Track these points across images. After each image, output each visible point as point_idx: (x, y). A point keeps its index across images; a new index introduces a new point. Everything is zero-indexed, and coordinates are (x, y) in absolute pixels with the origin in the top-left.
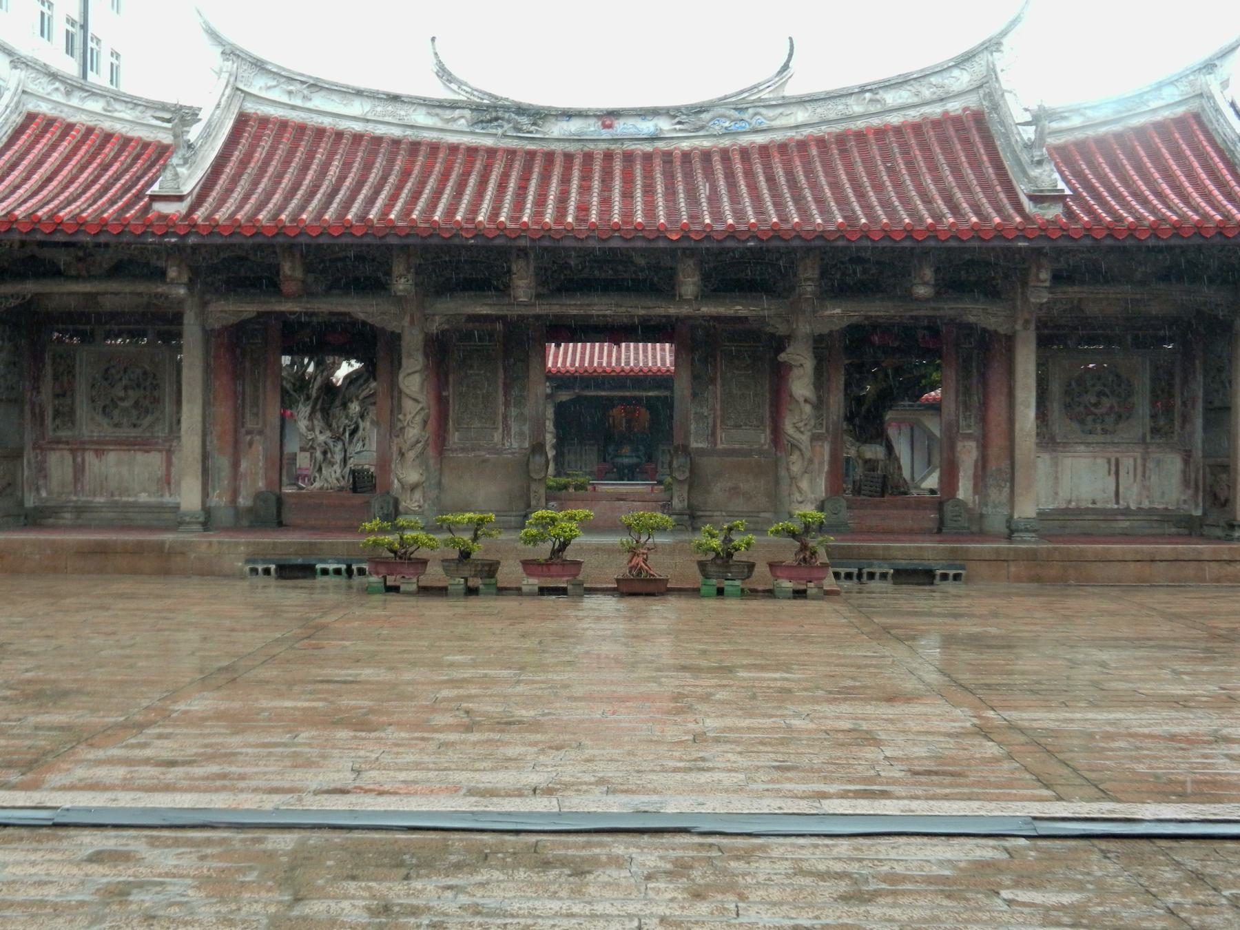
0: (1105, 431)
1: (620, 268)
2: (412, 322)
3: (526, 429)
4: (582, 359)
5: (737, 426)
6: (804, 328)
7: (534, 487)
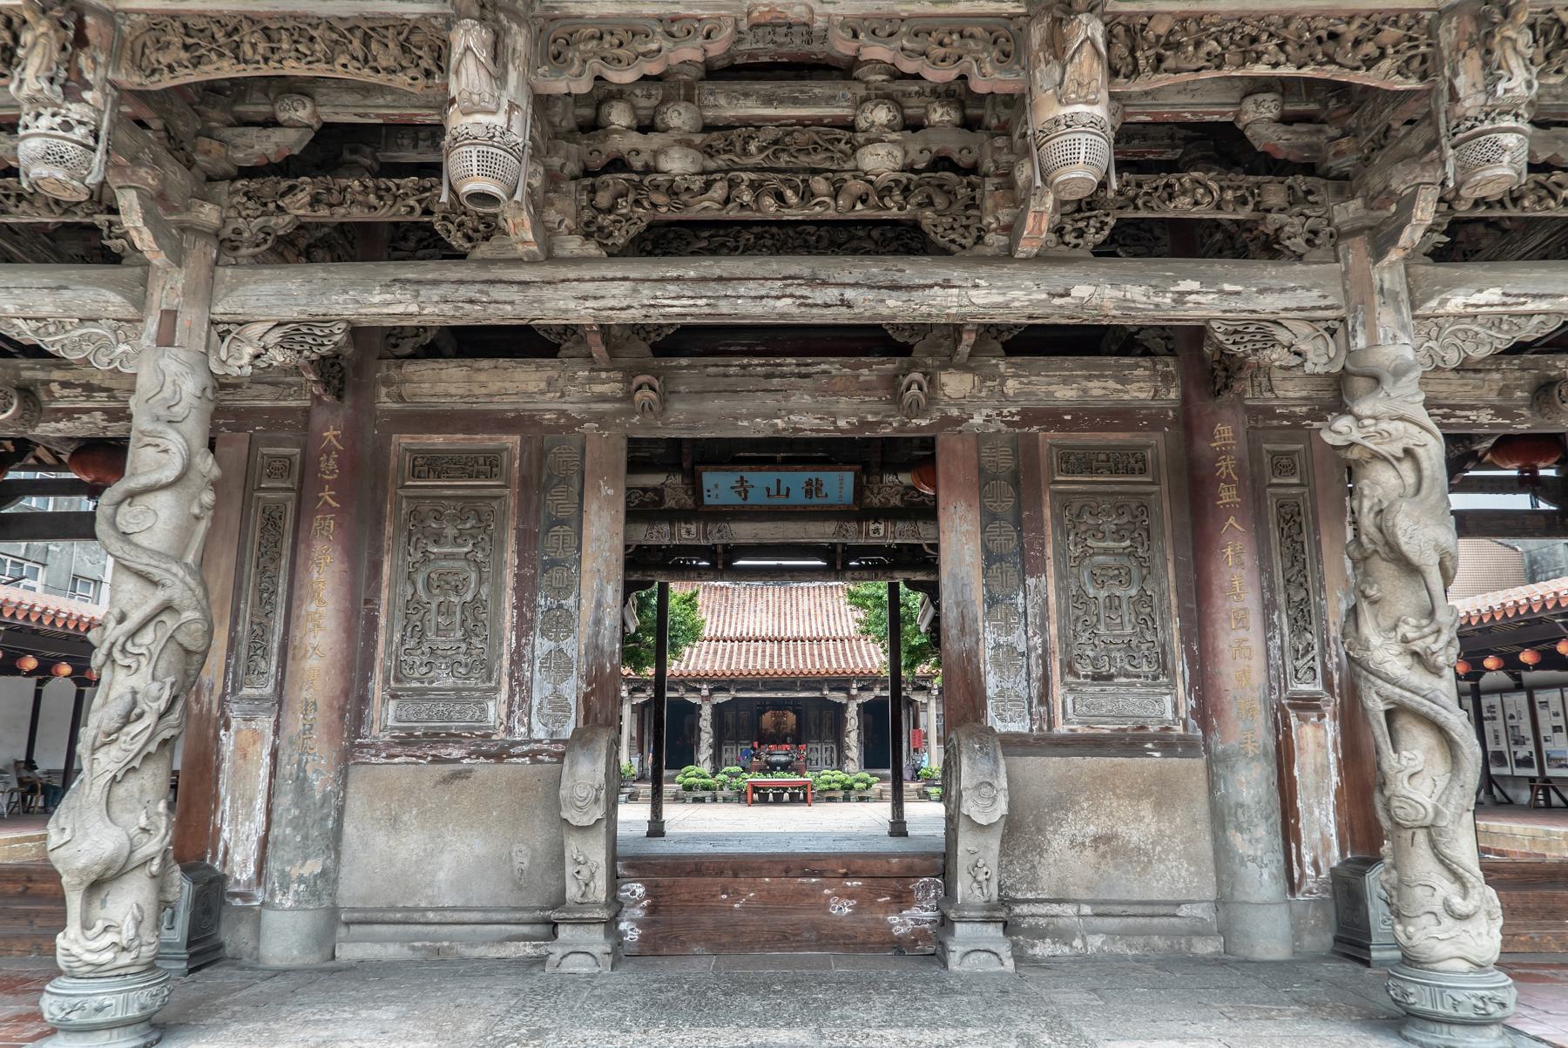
1: (820, 184)
2: (166, 338)
3: (572, 689)
4: (738, 663)
5: (1097, 677)
6: (1393, 341)
7: (573, 846)
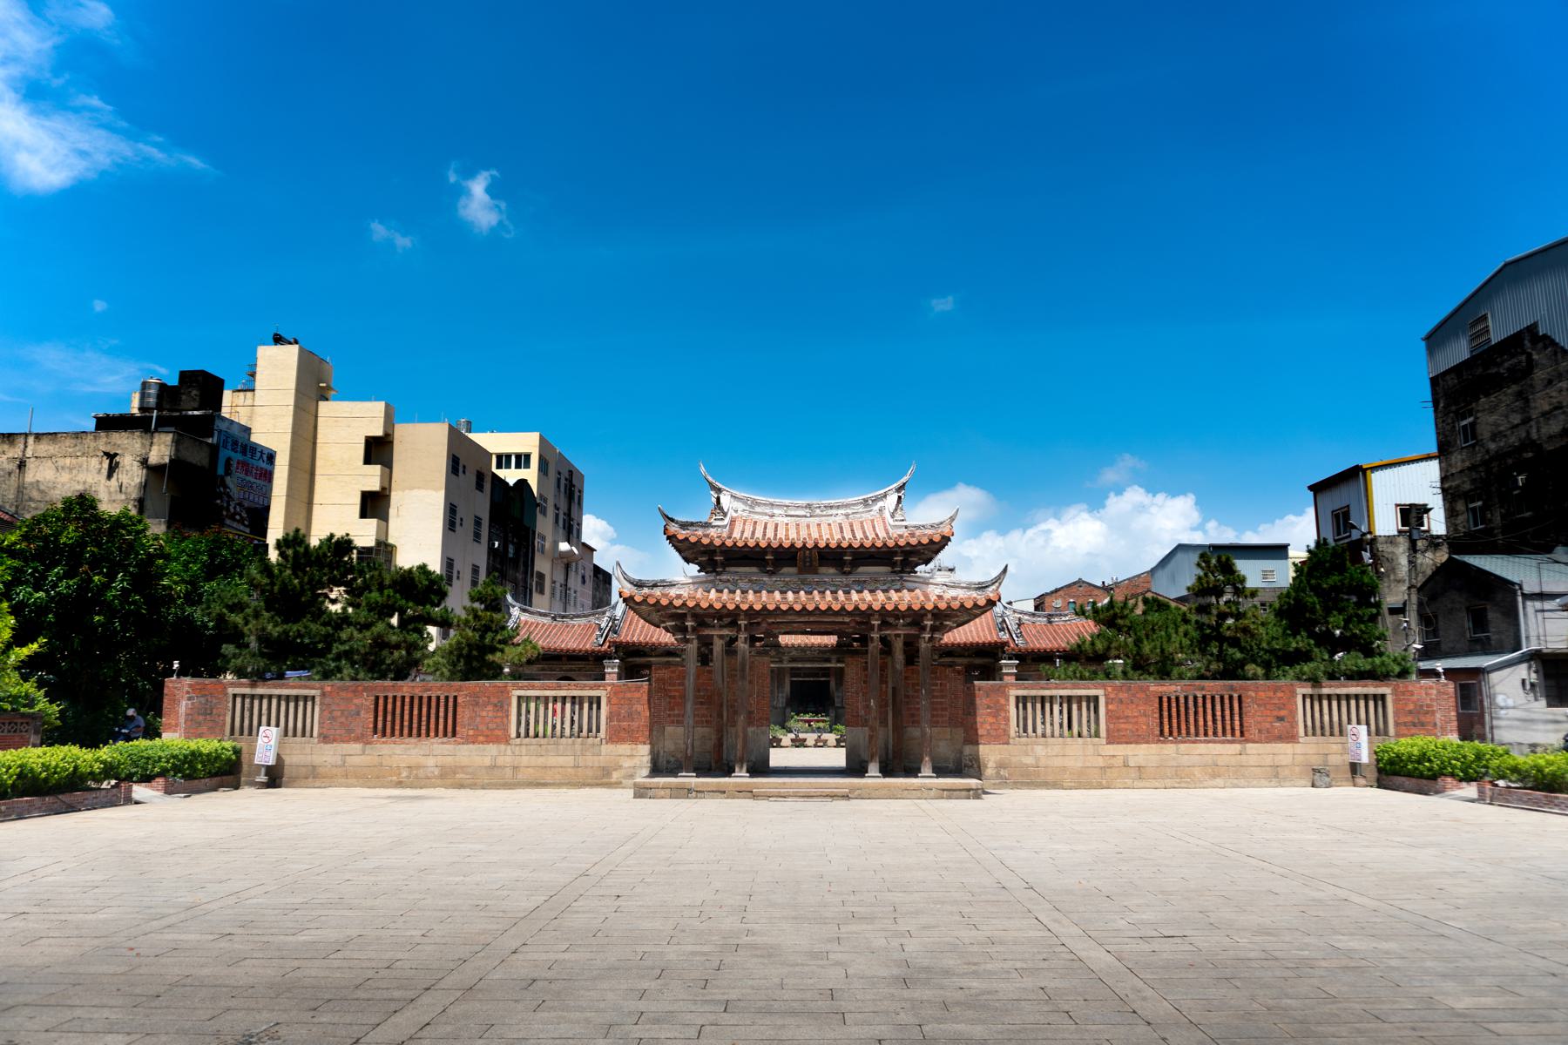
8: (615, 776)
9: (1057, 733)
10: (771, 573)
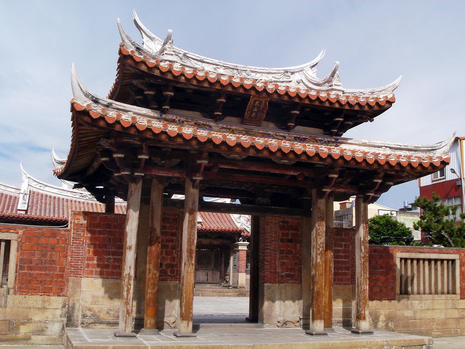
0: (206, 267)
8: (23, 330)
9: (427, 290)
10: (217, 119)
